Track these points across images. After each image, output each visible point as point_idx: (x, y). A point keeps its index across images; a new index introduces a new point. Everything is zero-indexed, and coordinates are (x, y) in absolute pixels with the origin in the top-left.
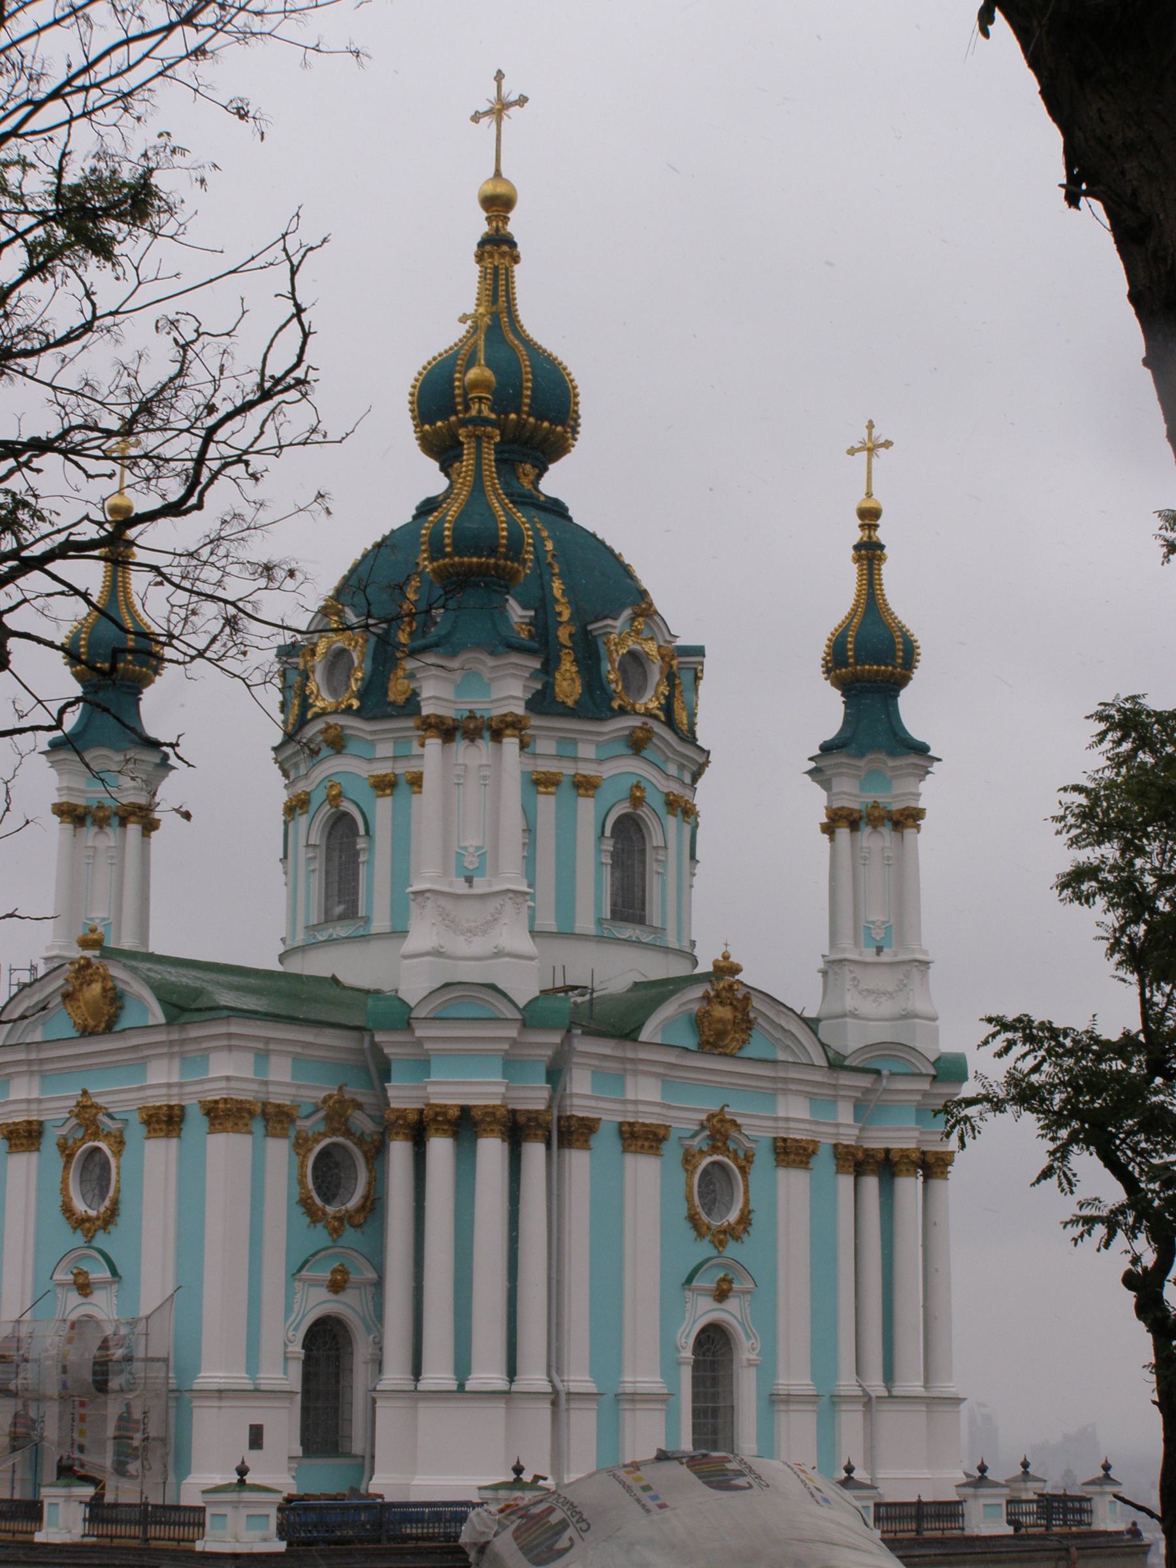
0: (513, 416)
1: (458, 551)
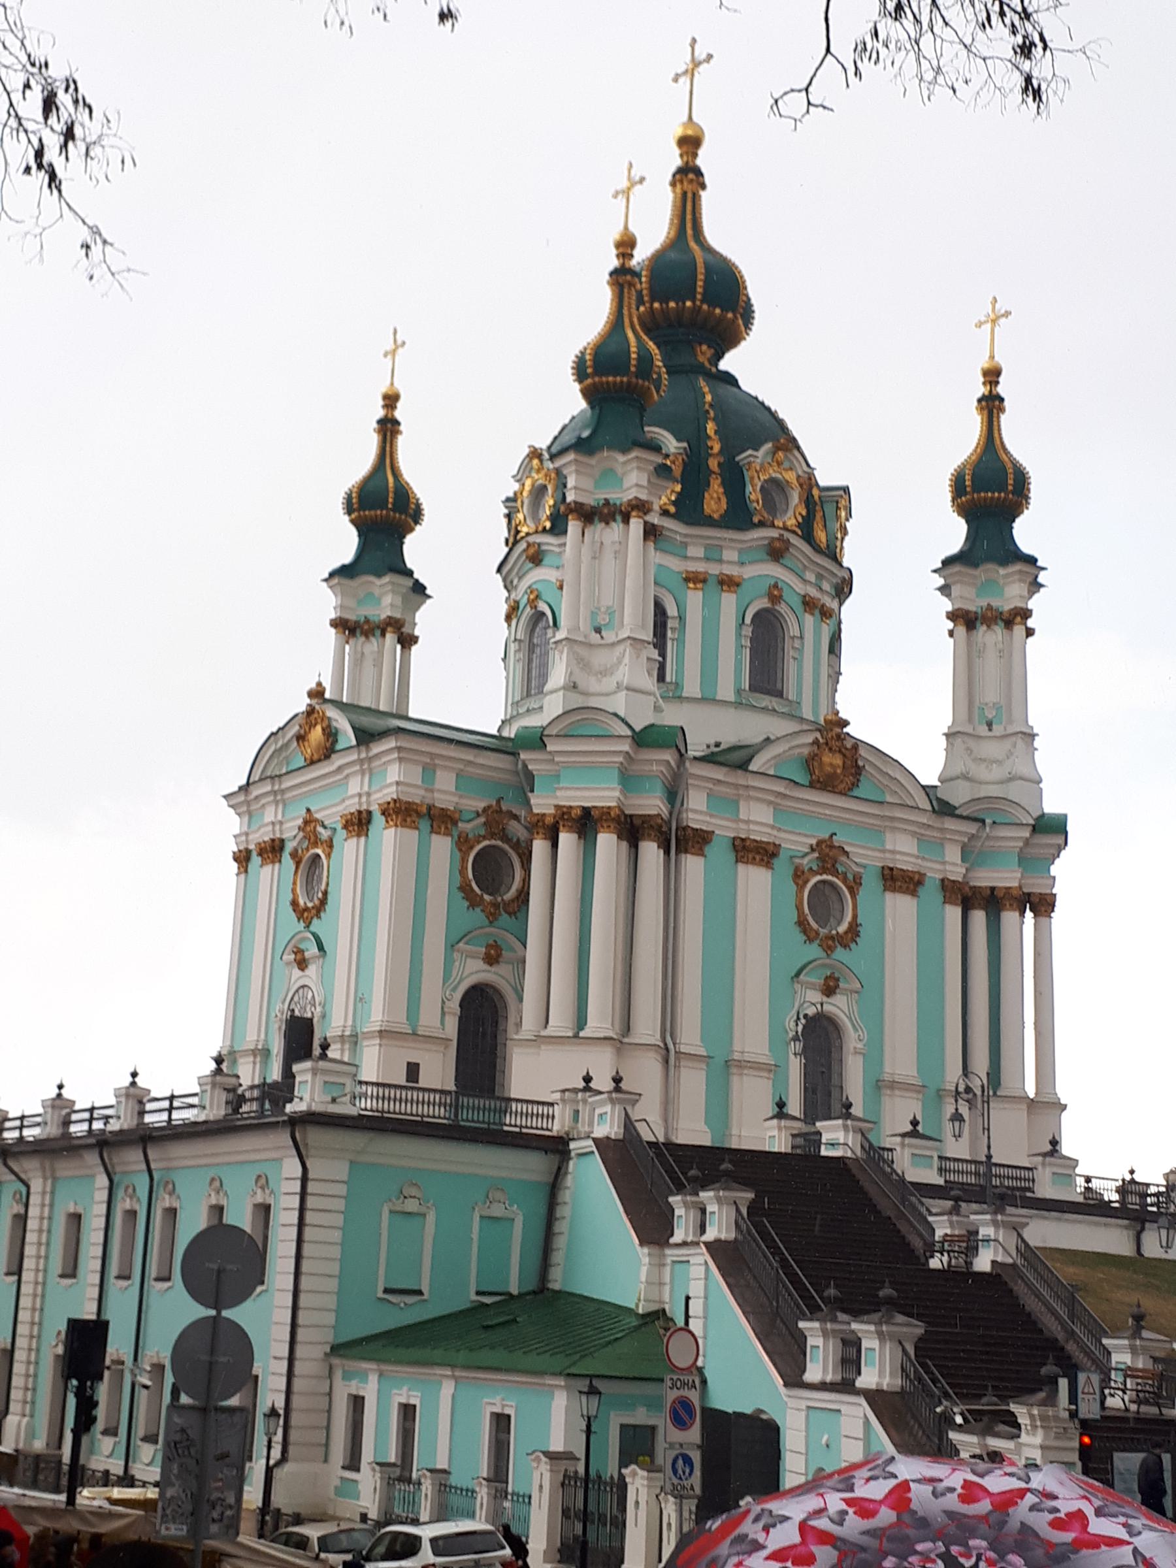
0: (688, 304)
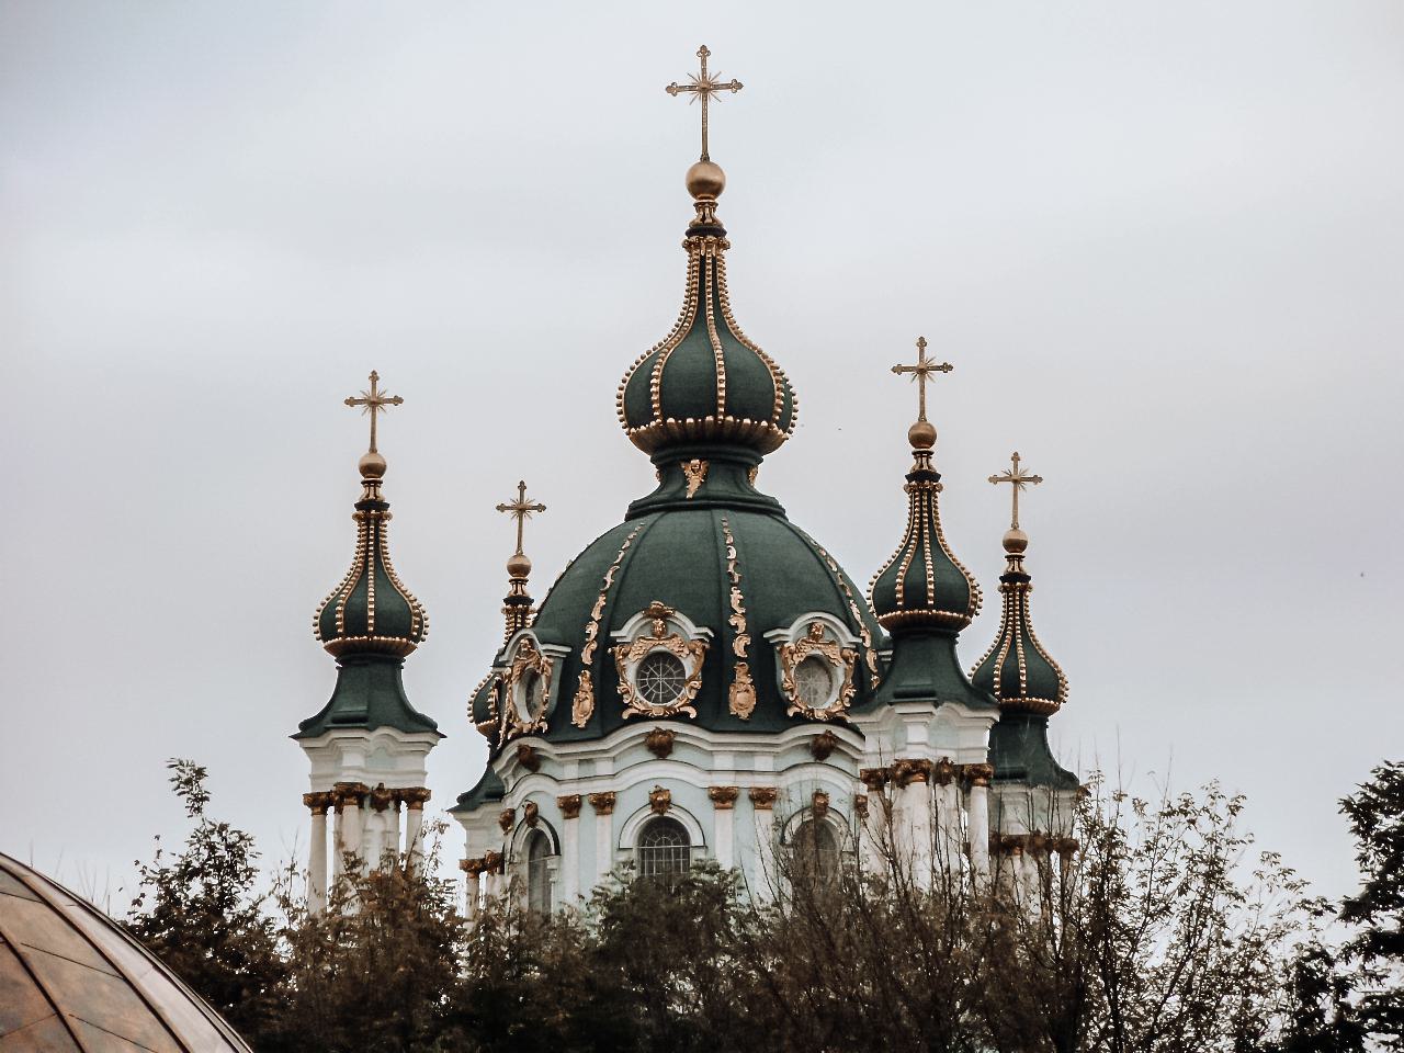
0: (710, 418)
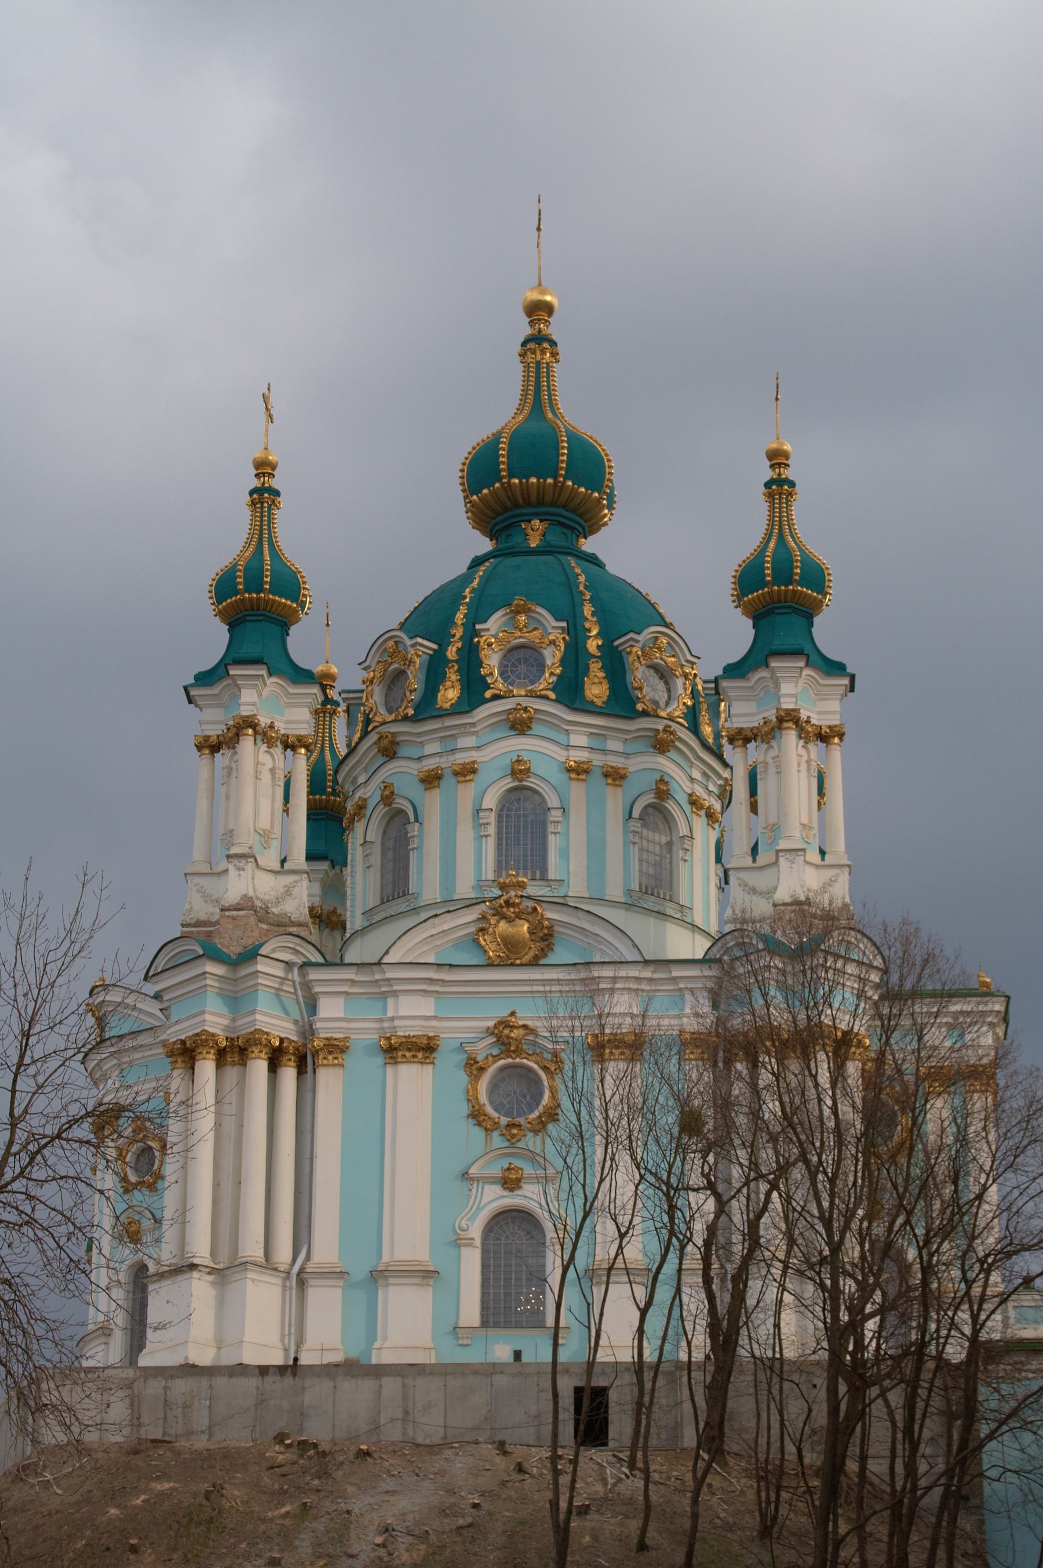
0: (497, 485)
1: (219, 602)
